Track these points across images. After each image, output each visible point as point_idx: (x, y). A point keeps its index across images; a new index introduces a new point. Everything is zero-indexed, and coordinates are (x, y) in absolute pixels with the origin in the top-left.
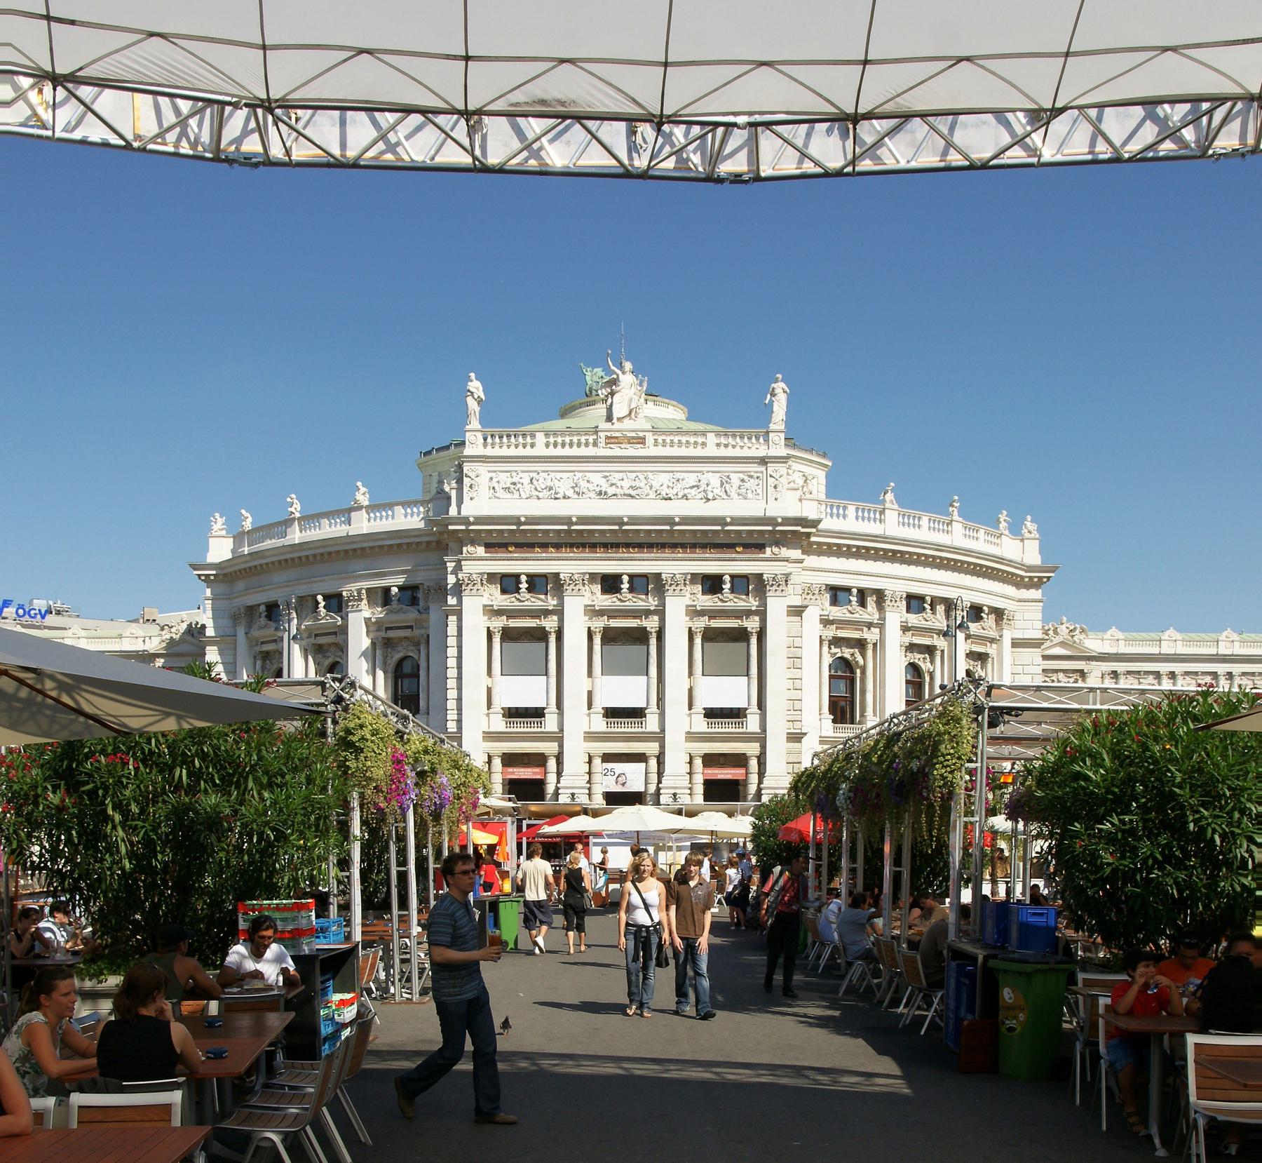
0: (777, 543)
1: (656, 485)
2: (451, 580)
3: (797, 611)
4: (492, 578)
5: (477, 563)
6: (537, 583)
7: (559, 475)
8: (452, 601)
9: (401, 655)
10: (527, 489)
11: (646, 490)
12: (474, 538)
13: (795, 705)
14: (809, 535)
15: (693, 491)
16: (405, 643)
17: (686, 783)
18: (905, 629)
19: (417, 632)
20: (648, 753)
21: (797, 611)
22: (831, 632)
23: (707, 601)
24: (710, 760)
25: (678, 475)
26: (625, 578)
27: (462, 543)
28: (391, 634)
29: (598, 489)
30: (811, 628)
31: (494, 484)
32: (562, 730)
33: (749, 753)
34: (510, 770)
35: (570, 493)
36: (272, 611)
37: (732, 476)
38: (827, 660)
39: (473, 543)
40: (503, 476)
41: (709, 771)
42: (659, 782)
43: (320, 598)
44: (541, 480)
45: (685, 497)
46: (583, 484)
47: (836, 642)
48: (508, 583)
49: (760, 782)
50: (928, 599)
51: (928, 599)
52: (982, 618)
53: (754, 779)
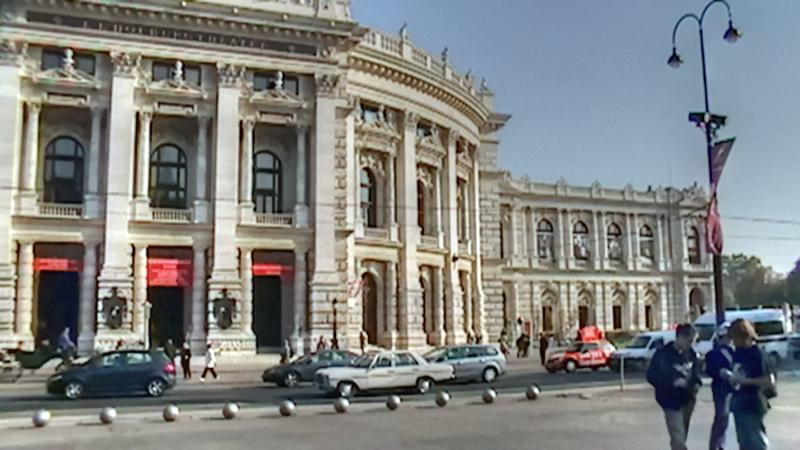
3: (344, 113)
13: (341, 206)
18: (418, 147)
22: (361, 143)
24: (258, 255)
34: (43, 261)
41: (256, 267)
47: (366, 151)
53: (301, 275)
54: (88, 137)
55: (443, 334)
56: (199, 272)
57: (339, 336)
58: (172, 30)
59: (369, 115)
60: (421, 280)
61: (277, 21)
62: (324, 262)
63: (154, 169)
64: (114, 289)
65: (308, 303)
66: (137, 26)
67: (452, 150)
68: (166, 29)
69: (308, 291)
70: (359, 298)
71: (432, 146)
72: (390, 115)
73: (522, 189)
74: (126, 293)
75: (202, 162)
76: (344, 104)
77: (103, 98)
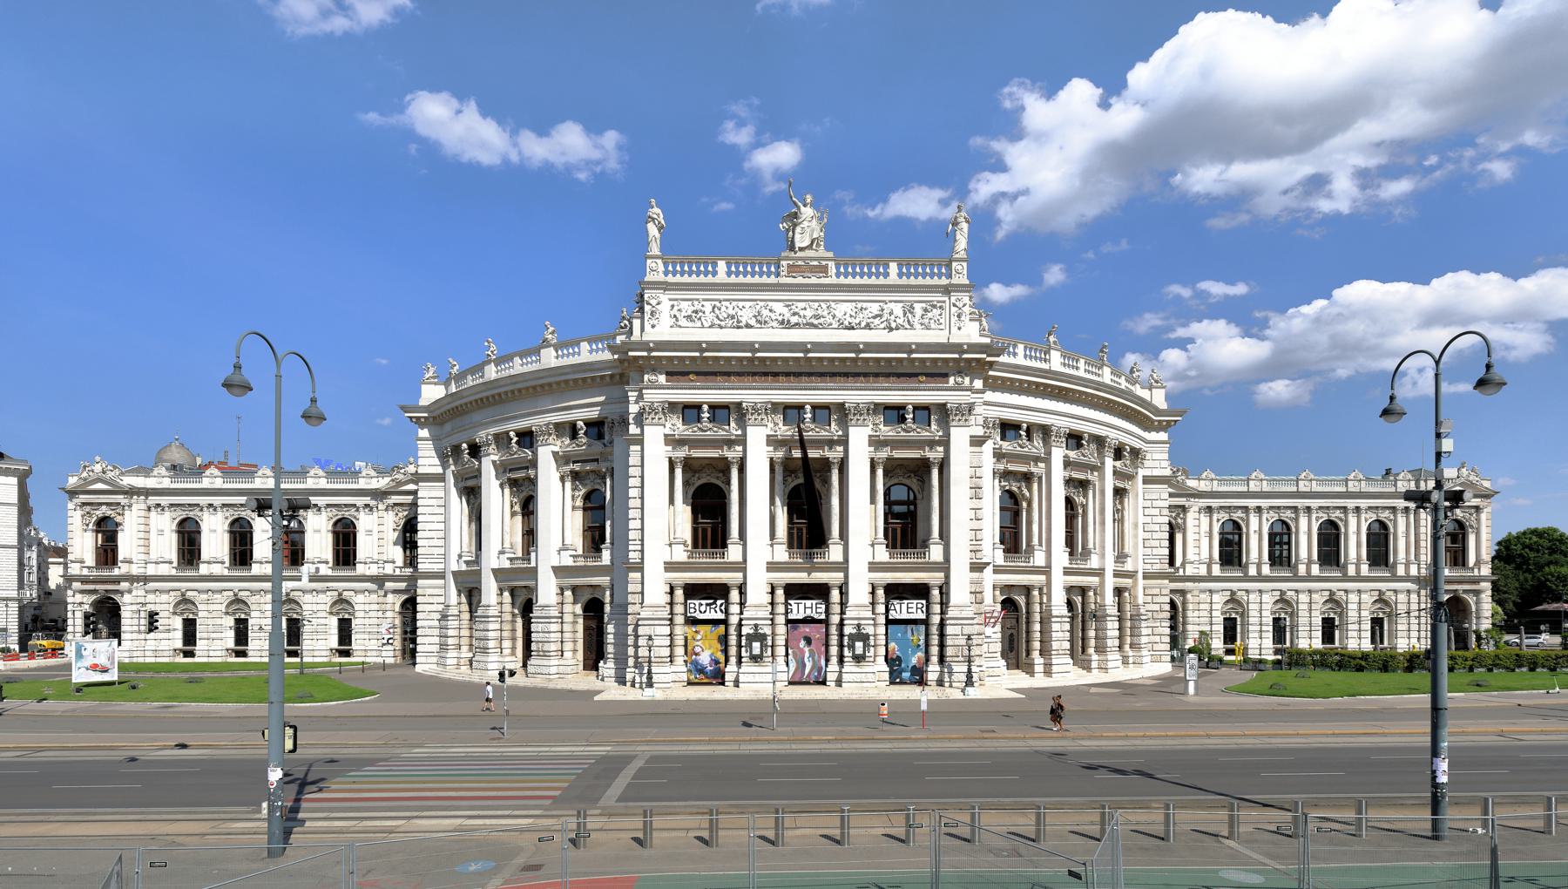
0: (960, 373)
1: (839, 315)
2: (634, 409)
3: (977, 442)
4: (672, 407)
5: (659, 391)
6: (720, 411)
7: (741, 304)
8: (633, 429)
10: (709, 317)
11: (829, 319)
12: (654, 366)
15: (877, 321)
17: (869, 614)
21: (977, 442)
22: (1001, 467)
23: (886, 431)
26: (808, 408)
27: (642, 372)
31: (675, 311)
32: (745, 561)
35: (753, 322)
38: (998, 493)
39: (654, 370)
40: (684, 305)
42: (843, 613)
45: (868, 327)
46: (765, 312)
48: (690, 411)
49: (942, 613)
55: (1095, 657)
56: (836, 609)
57: (974, 669)
60: (1070, 604)
62: (960, 594)
65: (942, 635)
69: (942, 625)
70: (998, 628)
74: (767, 630)
75: (835, 501)
76: (980, 431)
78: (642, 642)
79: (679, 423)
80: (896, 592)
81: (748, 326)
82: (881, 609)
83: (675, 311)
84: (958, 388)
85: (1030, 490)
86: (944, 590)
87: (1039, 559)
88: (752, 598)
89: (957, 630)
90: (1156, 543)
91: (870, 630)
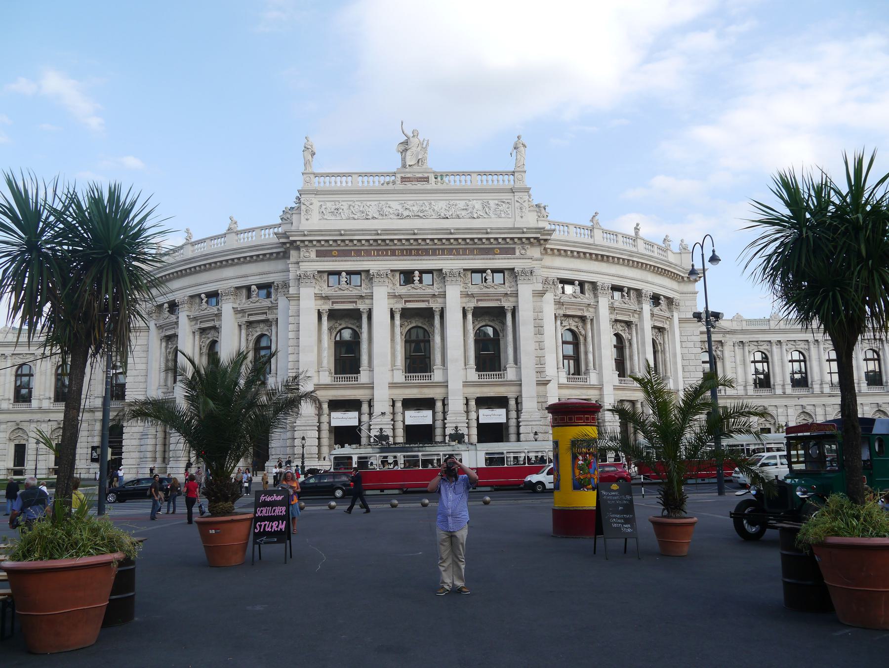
2: (292, 276)
3: (541, 294)
5: (311, 264)
7: (368, 203)
8: (292, 290)
9: (259, 333)
10: (346, 213)
13: (540, 361)
14: (546, 240)
15: (464, 213)
16: (262, 325)
18: (612, 309)
19: (270, 317)
20: (436, 397)
22: (562, 312)
25: (452, 203)
26: (417, 273)
28: (252, 318)
29: (396, 212)
30: (549, 309)
31: (323, 209)
33: (509, 395)
36: (173, 307)
37: (490, 202)
40: (329, 205)
42: (445, 419)
43: (203, 296)
44: (356, 207)
49: (518, 417)
50: (626, 289)
51: (626, 289)
52: (660, 304)
54: (360, 327)
58: (411, 250)
59: (569, 289)
61: (483, 233)
62: (530, 405)
63: (408, 345)
64: (381, 429)
66: (387, 250)
67: (647, 307)
68: (406, 250)
69: (518, 426)
71: (626, 306)
72: (586, 286)
73: (735, 326)
74: (390, 433)
75: (437, 339)
76: (539, 287)
77: (367, 301)
78: (298, 442)
79: (325, 286)
80: (484, 402)
81: (374, 218)
82: (473, 415)
83: (323, 209)
84: (523, 257)
85: (585, 329)
86: (518, 402)
87: (593, 378)
88: (378, 408)
89: (529, 429)
90: (693, 368)
91: (464, 431)
